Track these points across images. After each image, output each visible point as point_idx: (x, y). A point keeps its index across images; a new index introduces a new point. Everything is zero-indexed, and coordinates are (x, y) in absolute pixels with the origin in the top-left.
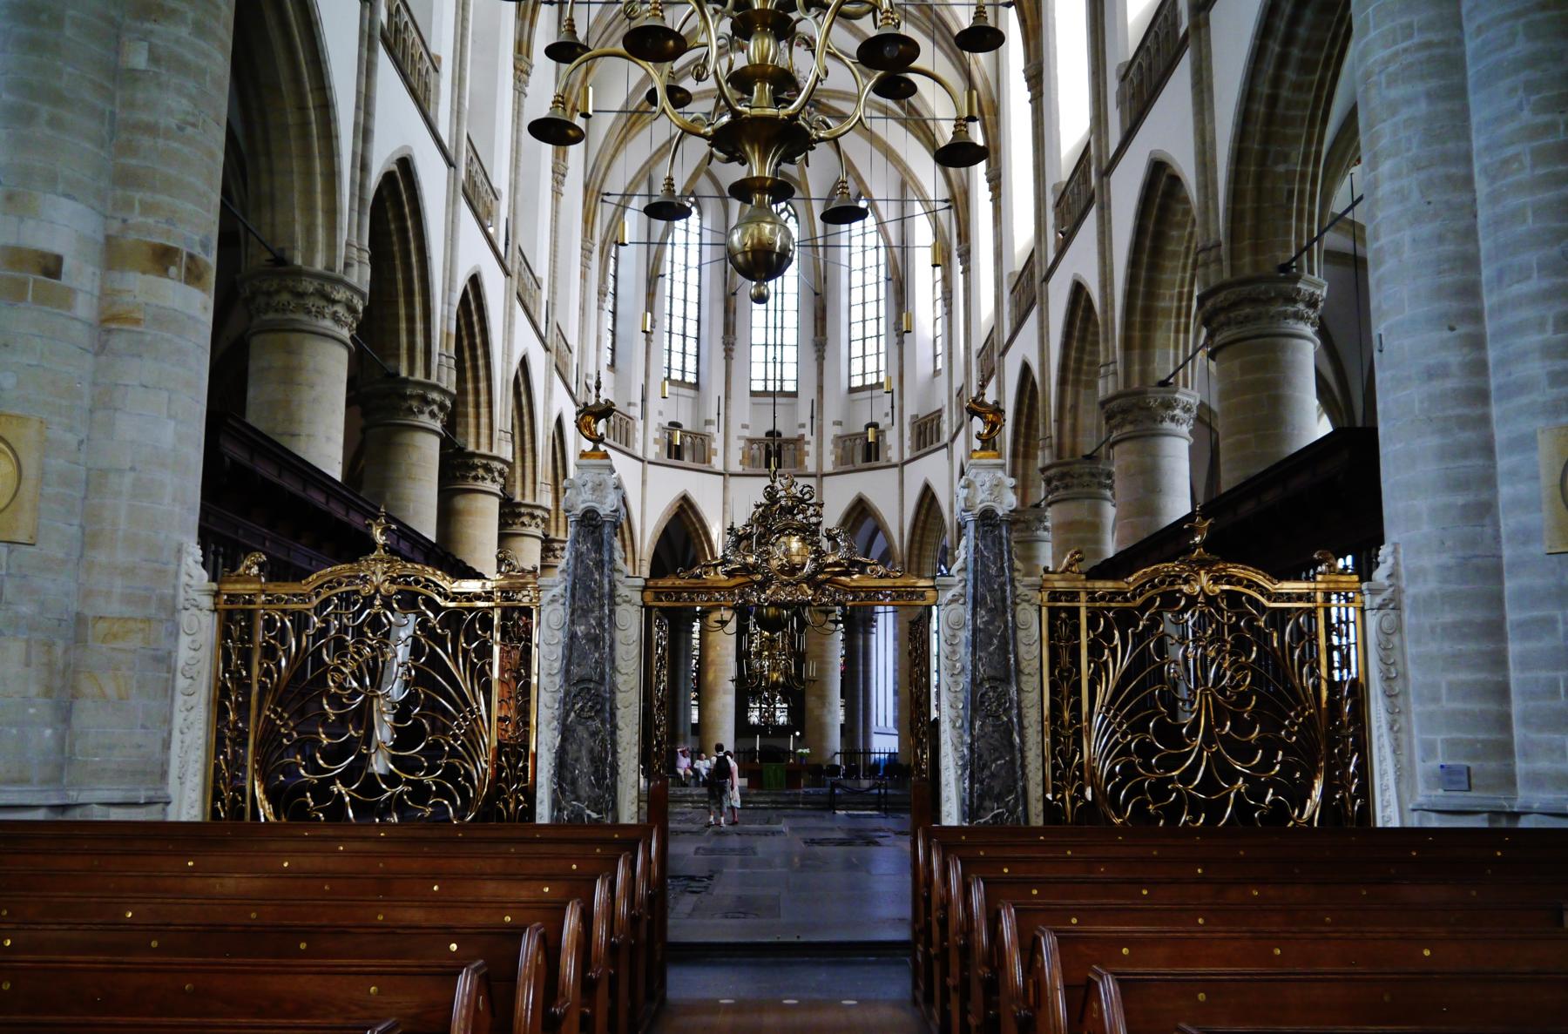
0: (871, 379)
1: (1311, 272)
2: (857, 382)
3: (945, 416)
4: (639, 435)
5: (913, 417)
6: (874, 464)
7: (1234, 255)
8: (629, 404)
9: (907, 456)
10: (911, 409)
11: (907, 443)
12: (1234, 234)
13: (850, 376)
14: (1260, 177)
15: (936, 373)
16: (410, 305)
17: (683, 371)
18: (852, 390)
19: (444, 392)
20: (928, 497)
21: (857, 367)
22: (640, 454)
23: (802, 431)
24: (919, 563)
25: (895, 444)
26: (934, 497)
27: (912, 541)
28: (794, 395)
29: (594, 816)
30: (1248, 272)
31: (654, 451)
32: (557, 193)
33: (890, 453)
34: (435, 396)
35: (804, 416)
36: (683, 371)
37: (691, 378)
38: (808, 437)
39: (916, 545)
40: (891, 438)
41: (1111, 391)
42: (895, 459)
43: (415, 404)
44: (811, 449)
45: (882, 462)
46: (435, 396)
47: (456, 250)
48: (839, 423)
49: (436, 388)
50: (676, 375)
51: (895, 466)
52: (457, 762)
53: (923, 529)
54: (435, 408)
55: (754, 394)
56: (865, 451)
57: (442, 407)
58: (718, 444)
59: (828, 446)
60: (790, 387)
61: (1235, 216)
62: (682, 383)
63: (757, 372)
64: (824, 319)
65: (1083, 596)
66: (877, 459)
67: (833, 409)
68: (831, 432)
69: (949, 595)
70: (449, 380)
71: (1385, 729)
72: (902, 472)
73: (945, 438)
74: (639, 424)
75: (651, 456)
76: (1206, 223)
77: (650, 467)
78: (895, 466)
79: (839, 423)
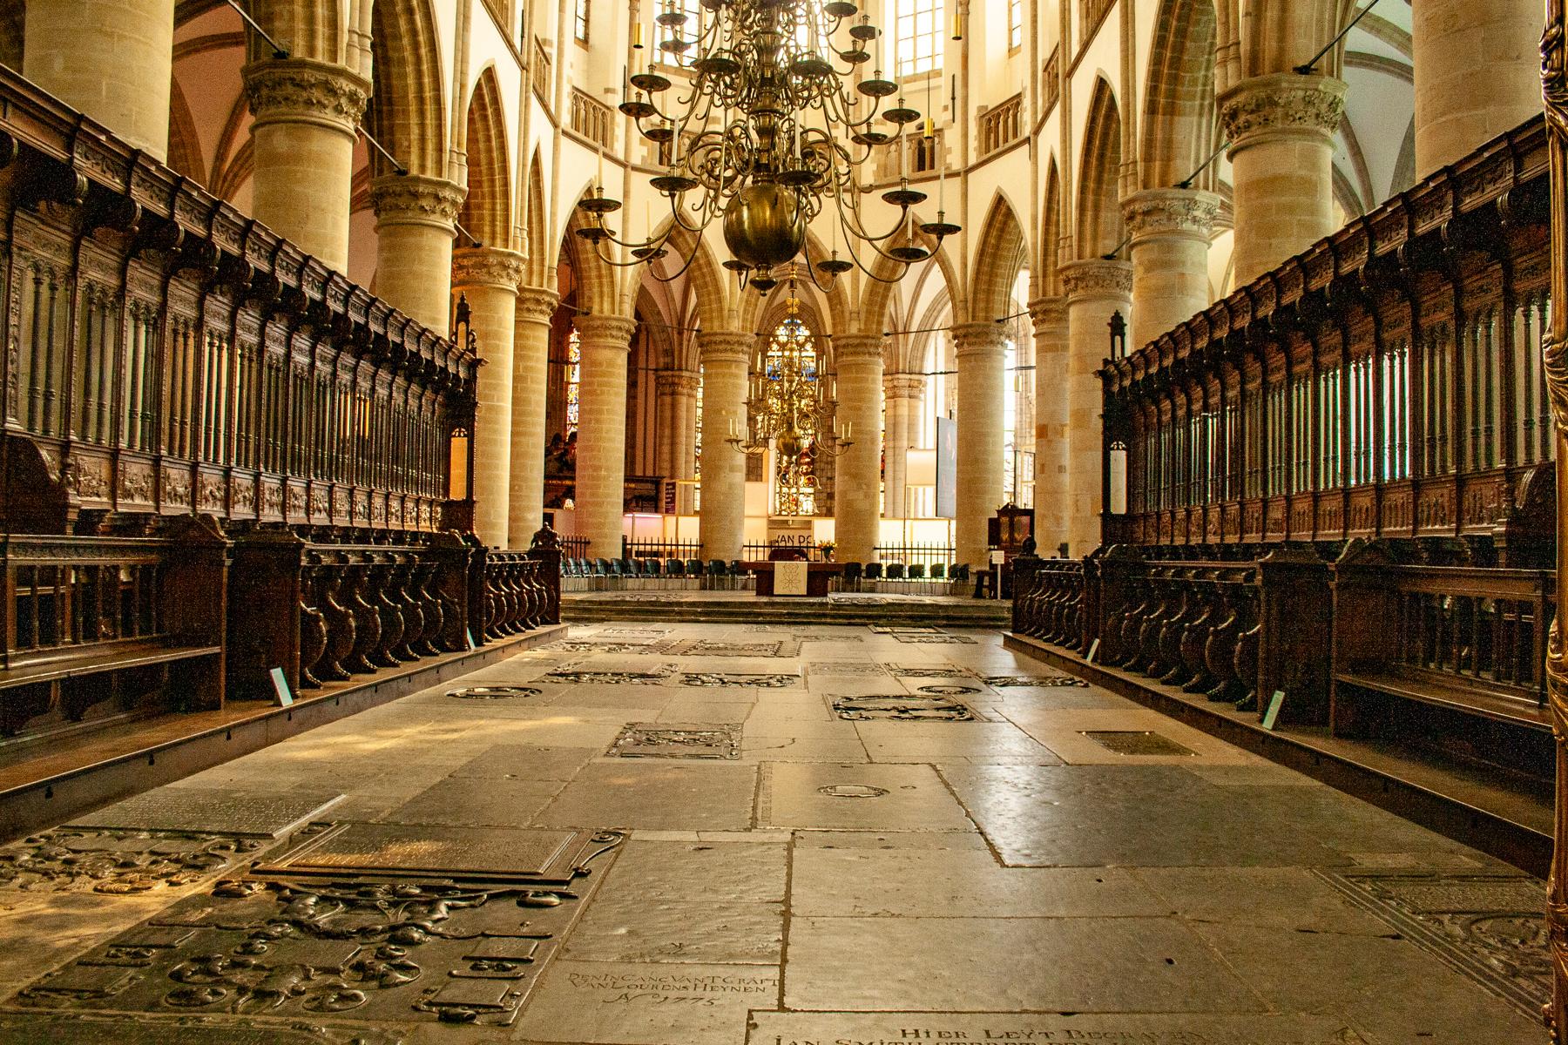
5: (981, 108)
6: (927, 173)
8: (607, 91)
9: (972, 161)
11: (973, 143)
20: (1001, 211)
22: (621, 157)
24: (988, 301)
26: (1009, 214)
27: (978, 272)
33: (949, 159)
39: (985, 278)
42: (957, 165)
45: (940, 169)
51: (957, 174)
53: (995, 256)
66: (932, 167)
72: (966, 182)
75: (636, 160)
78: (957, 174)
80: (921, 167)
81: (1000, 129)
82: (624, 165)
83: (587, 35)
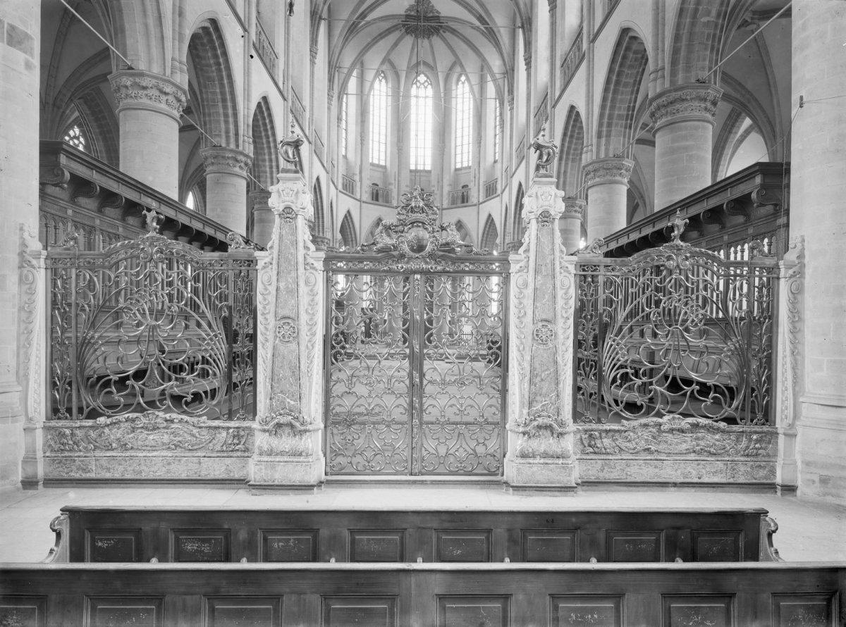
0: (465, 165)
1: (715, 83)
2: (459, 166)
3: (499, 182)
4: (358, 190)
7: (673, 74)
9: (481, 201)
12: (674, 63)
14: (693, 24)
15: (495, 162)
16: (225, 107)
17: (379, 159)
18: (456, 170)
19: (247, 156)
21: (459, 159)
22: (358, 198)
23: (433, 189)
25: (476, 194)
28: (430, 172)
29: (292, 403)
30: (680, 82)
31: (366, 197)
32: (313, 63)
34: (241, 158)
35: (434, 182)
36: (379, 159)
37: (382, 163)
41: (589, 161)
43: (231, 162)
45: (469, 203)
46: (241, 158)
47: (252, 83)
49: (242, 153)
50: (376, 162)
51: (475, 205)
52: (206, 367)
54: (242, 165)
55: (411, 171)
57: (246, 164)
58: (394, 194)
60: (428, 168)
61: (675, 51)
62: (378, 166)
65: (602, 268)
68: (446, 189)
69: (518, 267)
70: (250, 150)
71: (788, 353)
73: (499, 192)
74: (358, 184)
76: (656, 60)
77: (364, 205)
78: (475, 205)
80: (463, 202)
81: (491, 191)
82: (360, 201)
83: (346, 153)
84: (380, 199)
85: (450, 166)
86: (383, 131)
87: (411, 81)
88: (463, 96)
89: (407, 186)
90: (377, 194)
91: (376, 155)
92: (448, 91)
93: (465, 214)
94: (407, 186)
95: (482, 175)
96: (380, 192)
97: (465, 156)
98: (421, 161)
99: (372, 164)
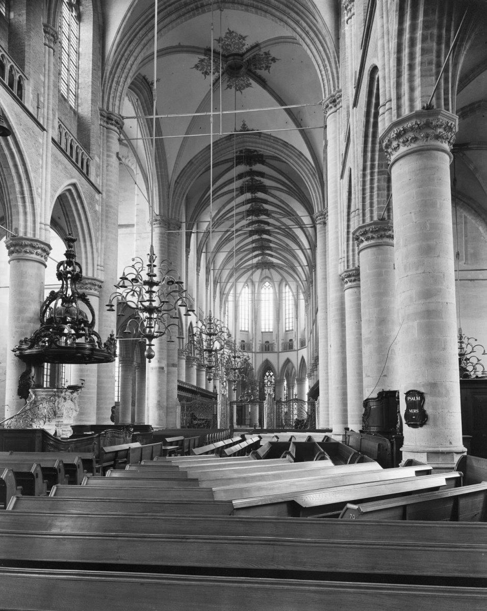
0: (291, 329)
2: (287, 329)
9: (299, 348)
10: (299, 338)
11: (299, 345)
13: (286, 328)
18: (286, 331)
25: (296, 345)
28: (272, 332)
35: (274, 338)
38: (275, 343)
40: (295, 344)
42: (296, 349)
44: (276, 346)
48: (283, 340)
55: (262, 332)
56: (289, 347)
59: (280, 345)
60: (271, 330)
63: (263, 327)
64: (279, 314)
66: (292, 349)
67: (281, 337)
68: (281, 342)
79: (283, 340)
80: (290, 349)
84: (246, 349)
85: (283, 329)
86: (247, 313)
87: (260, 287)
88: (288, 294)
89: (260, 341)
90: (244, 346)
91: (243, 326)
92: (280, 292)
93: (292, 355)
94: (260, 341)
95: (299, 335)
96: (245, 345)
97: (291, 324)
98: (267, 327)
99: (241, 331)
